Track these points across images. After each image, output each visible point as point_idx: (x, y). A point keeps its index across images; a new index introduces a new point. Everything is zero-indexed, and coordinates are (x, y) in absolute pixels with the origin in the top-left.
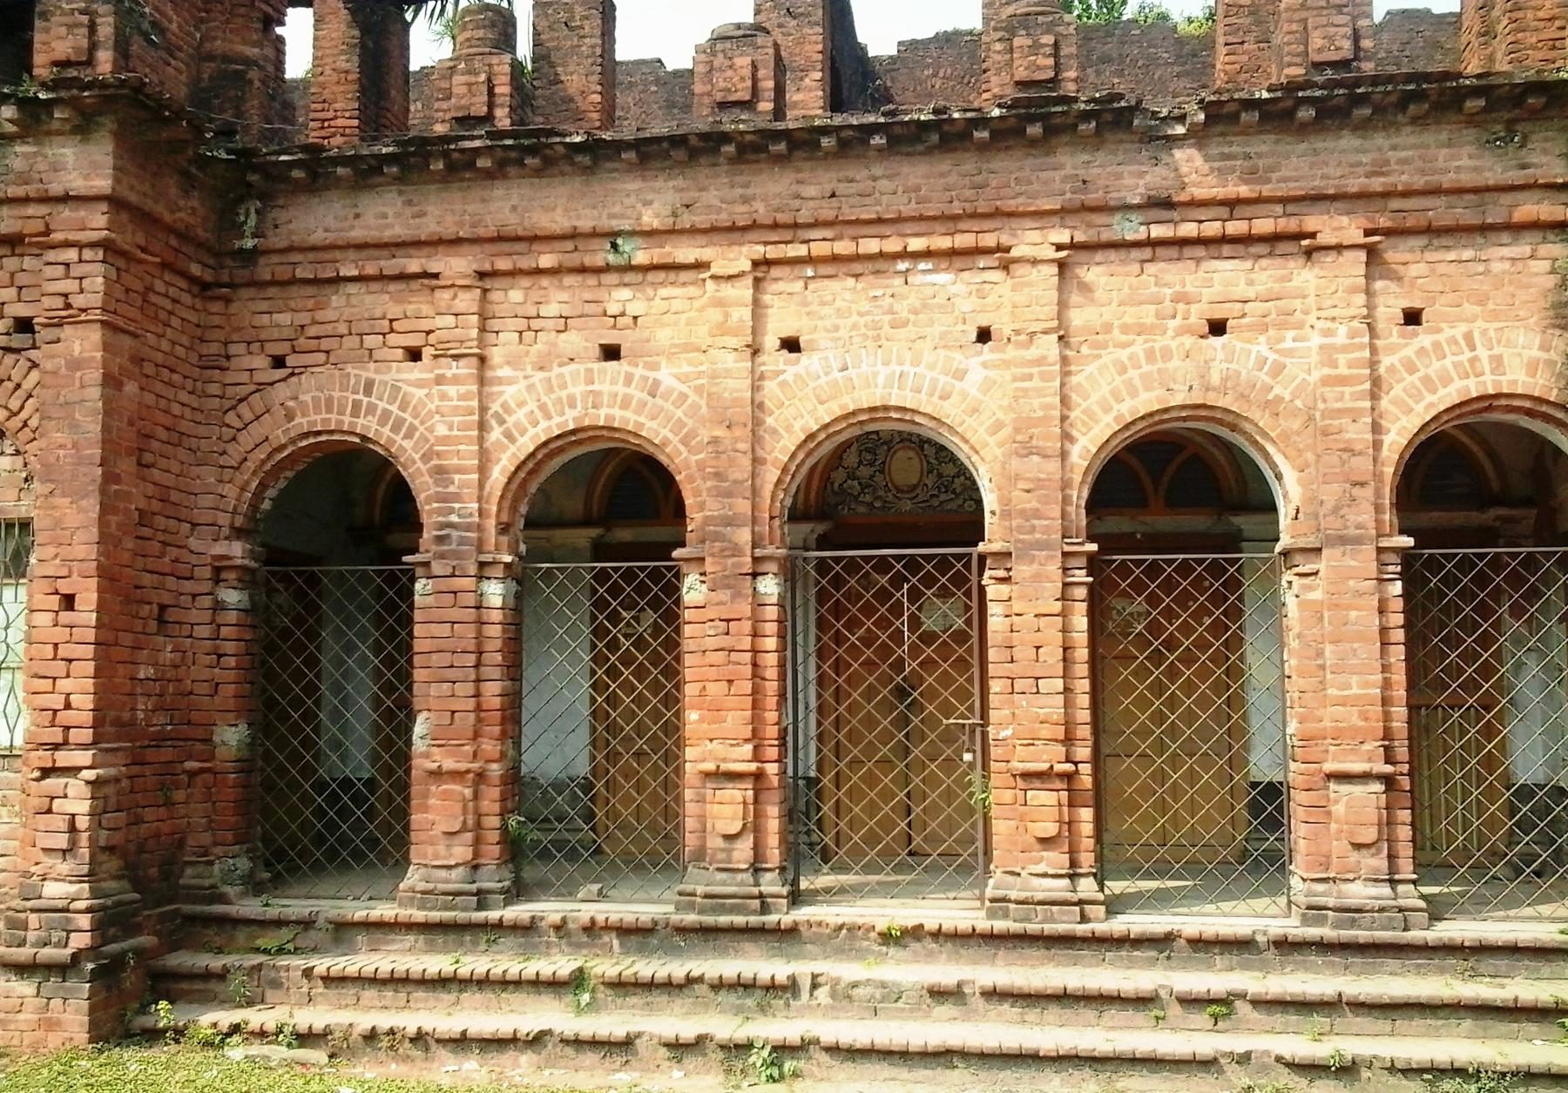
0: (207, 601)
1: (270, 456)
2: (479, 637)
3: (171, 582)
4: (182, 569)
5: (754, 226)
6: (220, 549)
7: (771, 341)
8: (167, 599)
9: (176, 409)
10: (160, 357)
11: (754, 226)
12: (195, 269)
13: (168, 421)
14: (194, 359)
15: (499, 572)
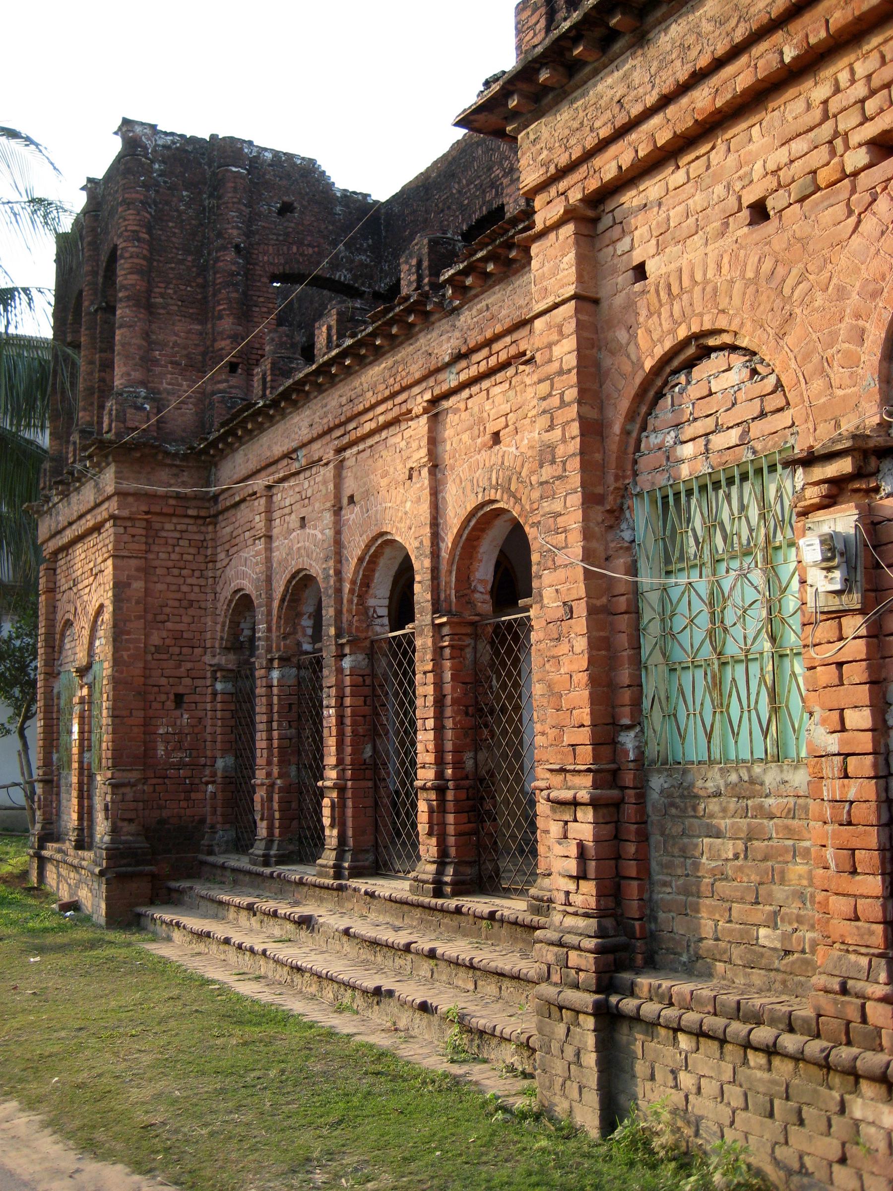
0: (210, 690)
1: (229, 605)
2: (270, 705)
3: (187, 681)
4: (194, 673)
5: (330, 430)
6: (215, 661)
7: (345, 501)
8: (181, 690)
9: (185, 588)
10: (170, 564)
11: (330, 430)
12: (191, 512)
13: (179, 596)
14: (200, 558)
15: (276, 664)
